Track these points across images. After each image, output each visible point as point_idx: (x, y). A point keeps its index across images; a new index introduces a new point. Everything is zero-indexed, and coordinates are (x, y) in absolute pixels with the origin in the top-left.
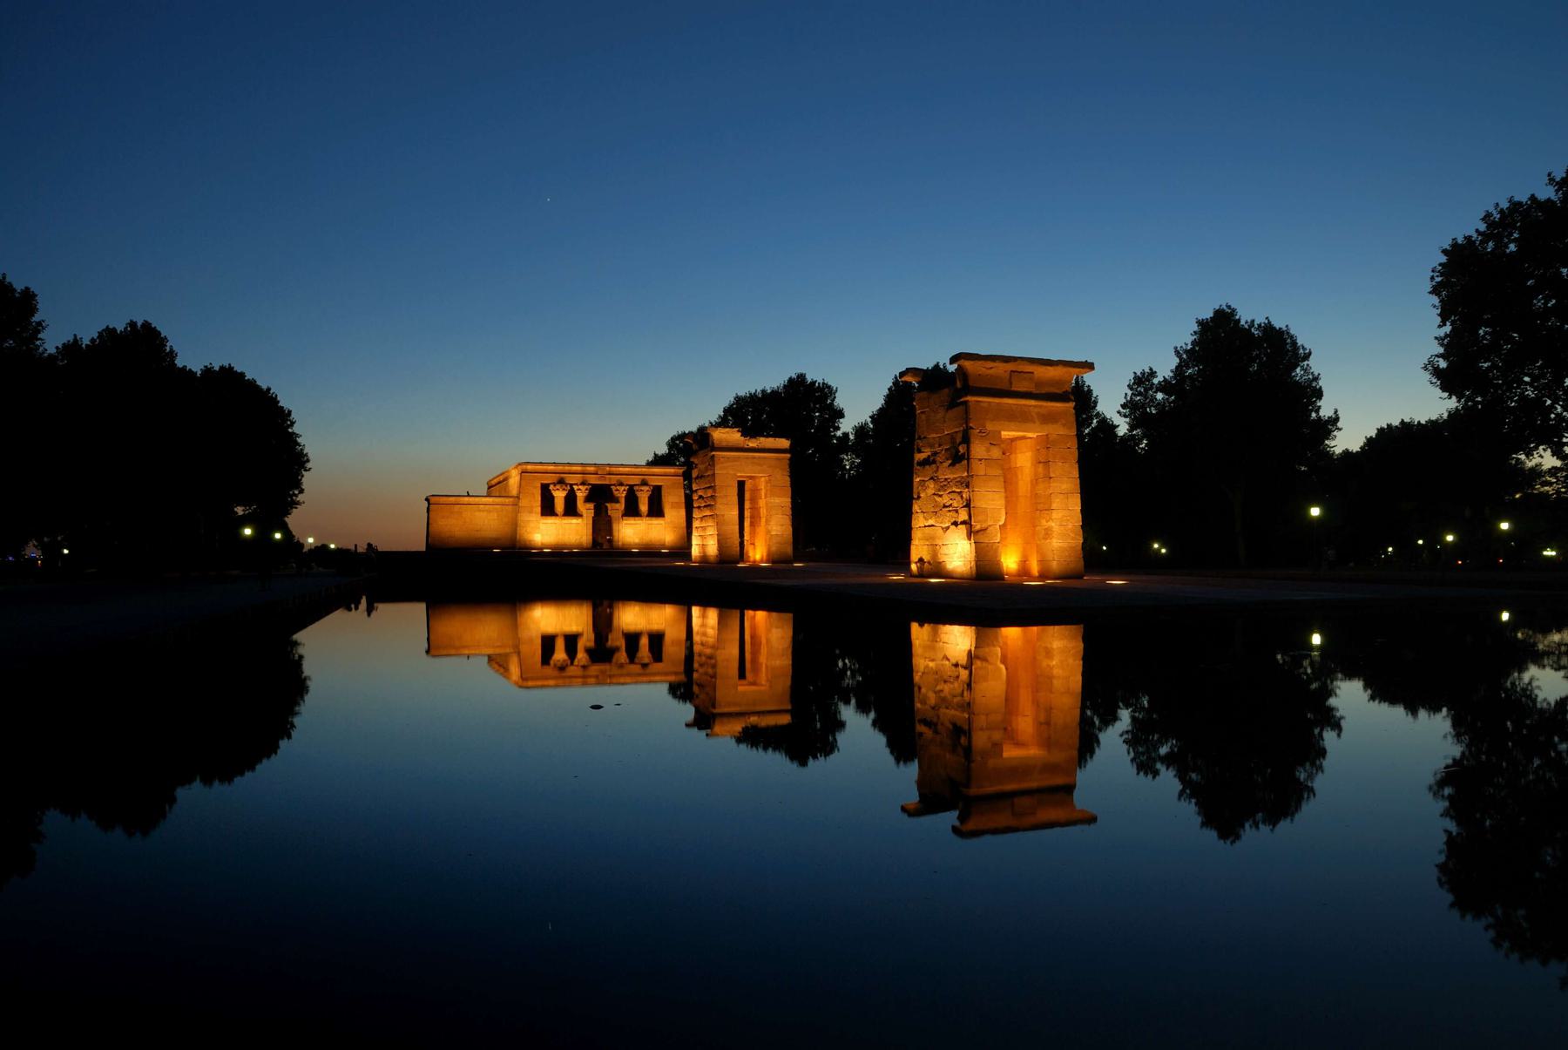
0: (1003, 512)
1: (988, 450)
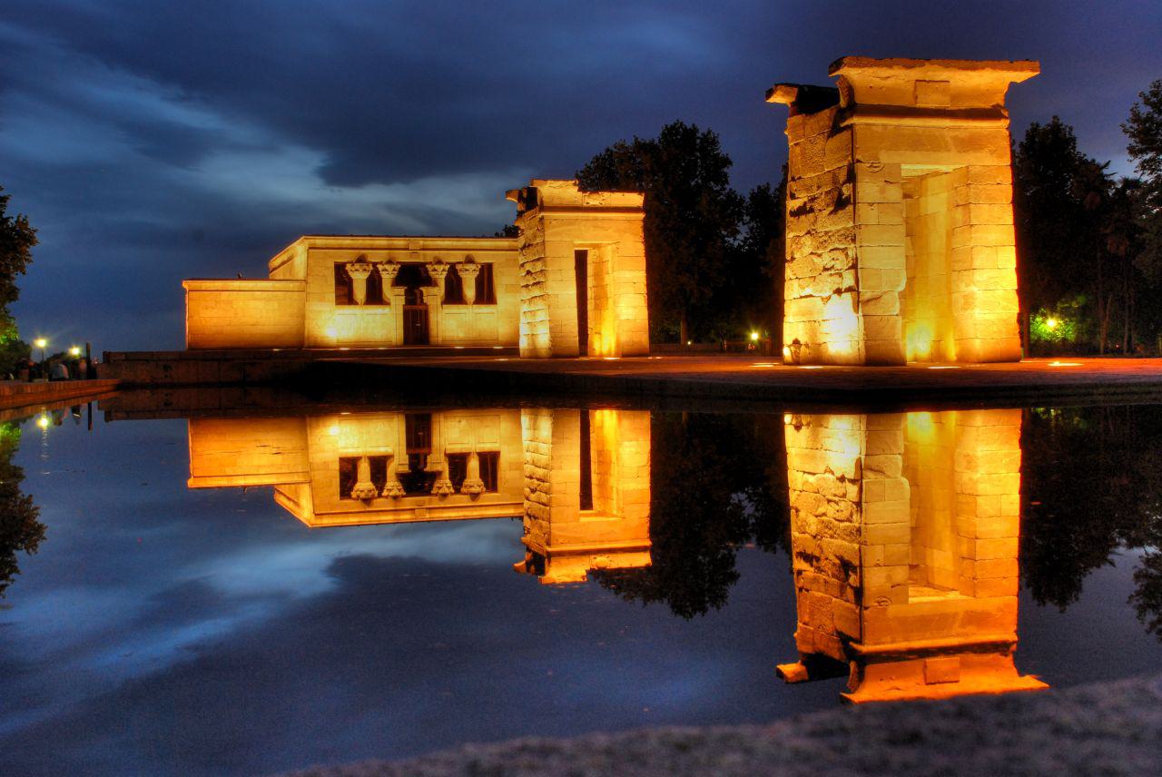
1: (882, 191)
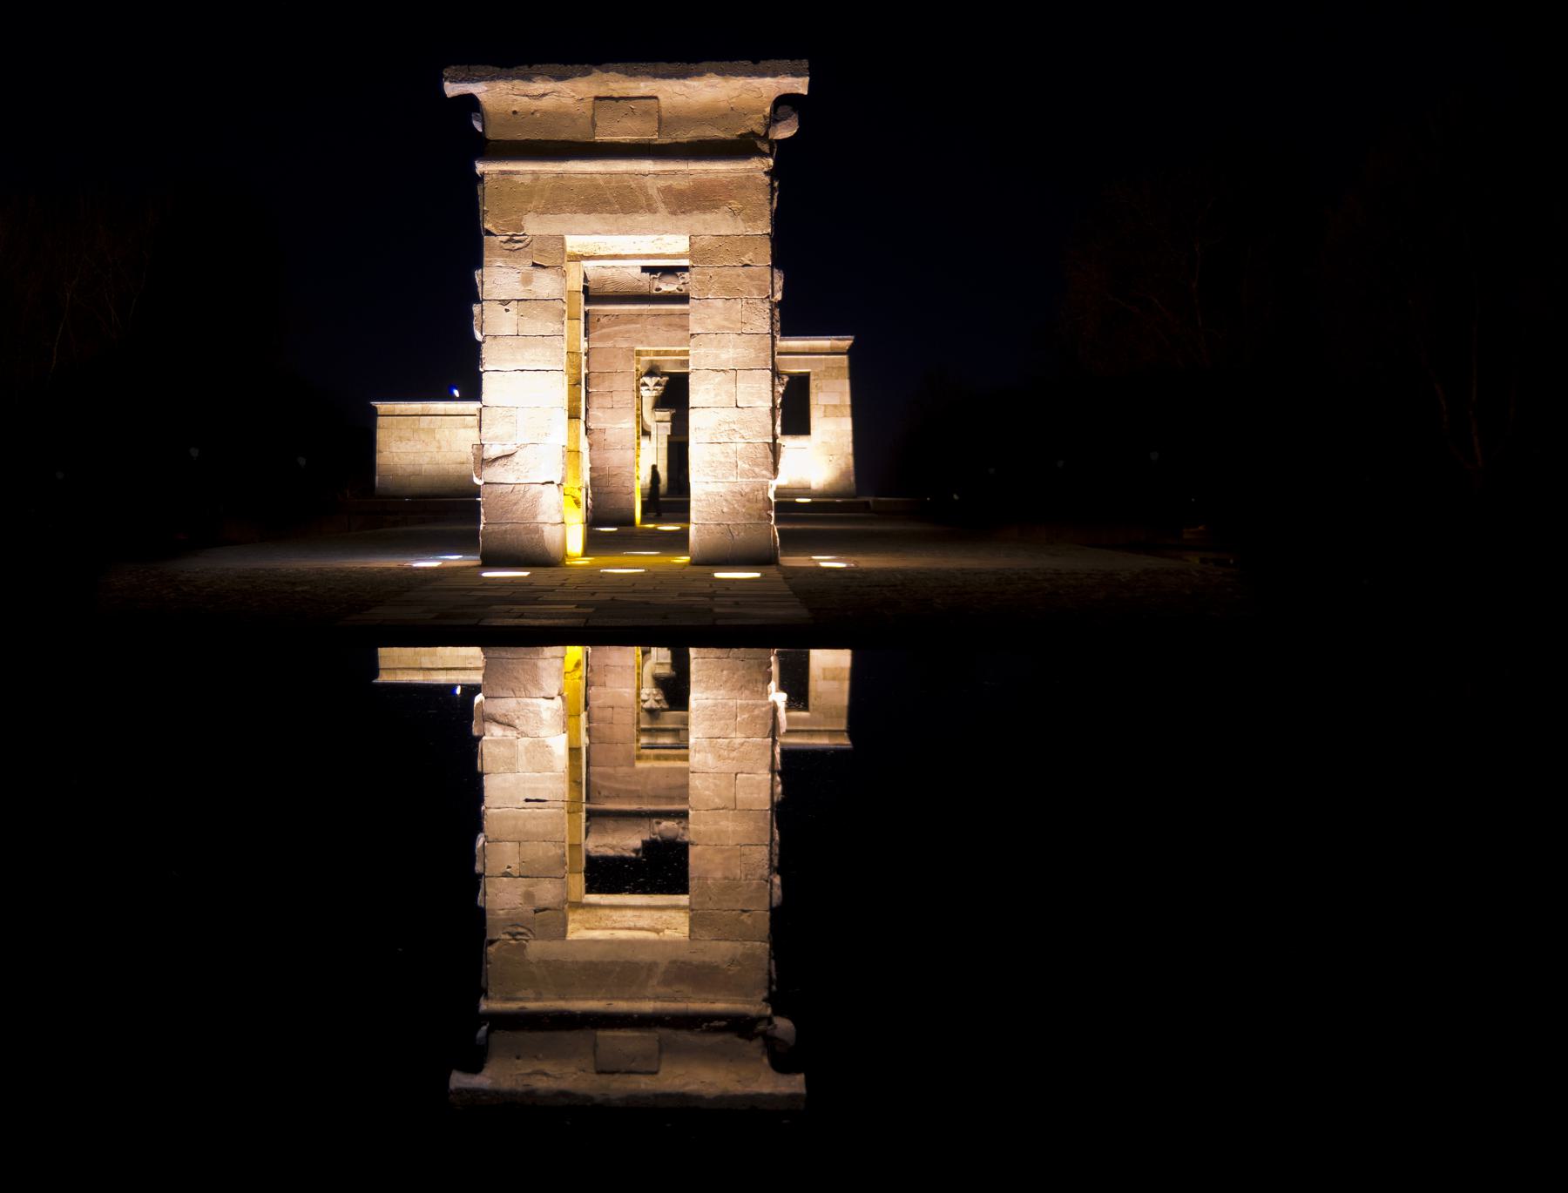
1: (527, 280)
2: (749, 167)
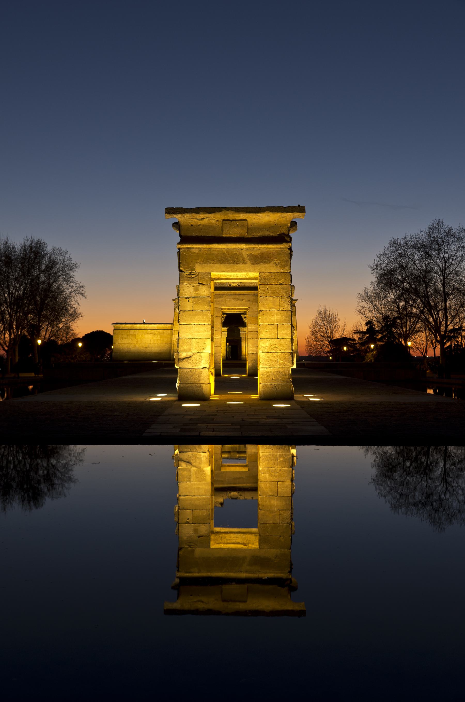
0: (209, 341)
1: (196, 290)
2: (282, 247)
